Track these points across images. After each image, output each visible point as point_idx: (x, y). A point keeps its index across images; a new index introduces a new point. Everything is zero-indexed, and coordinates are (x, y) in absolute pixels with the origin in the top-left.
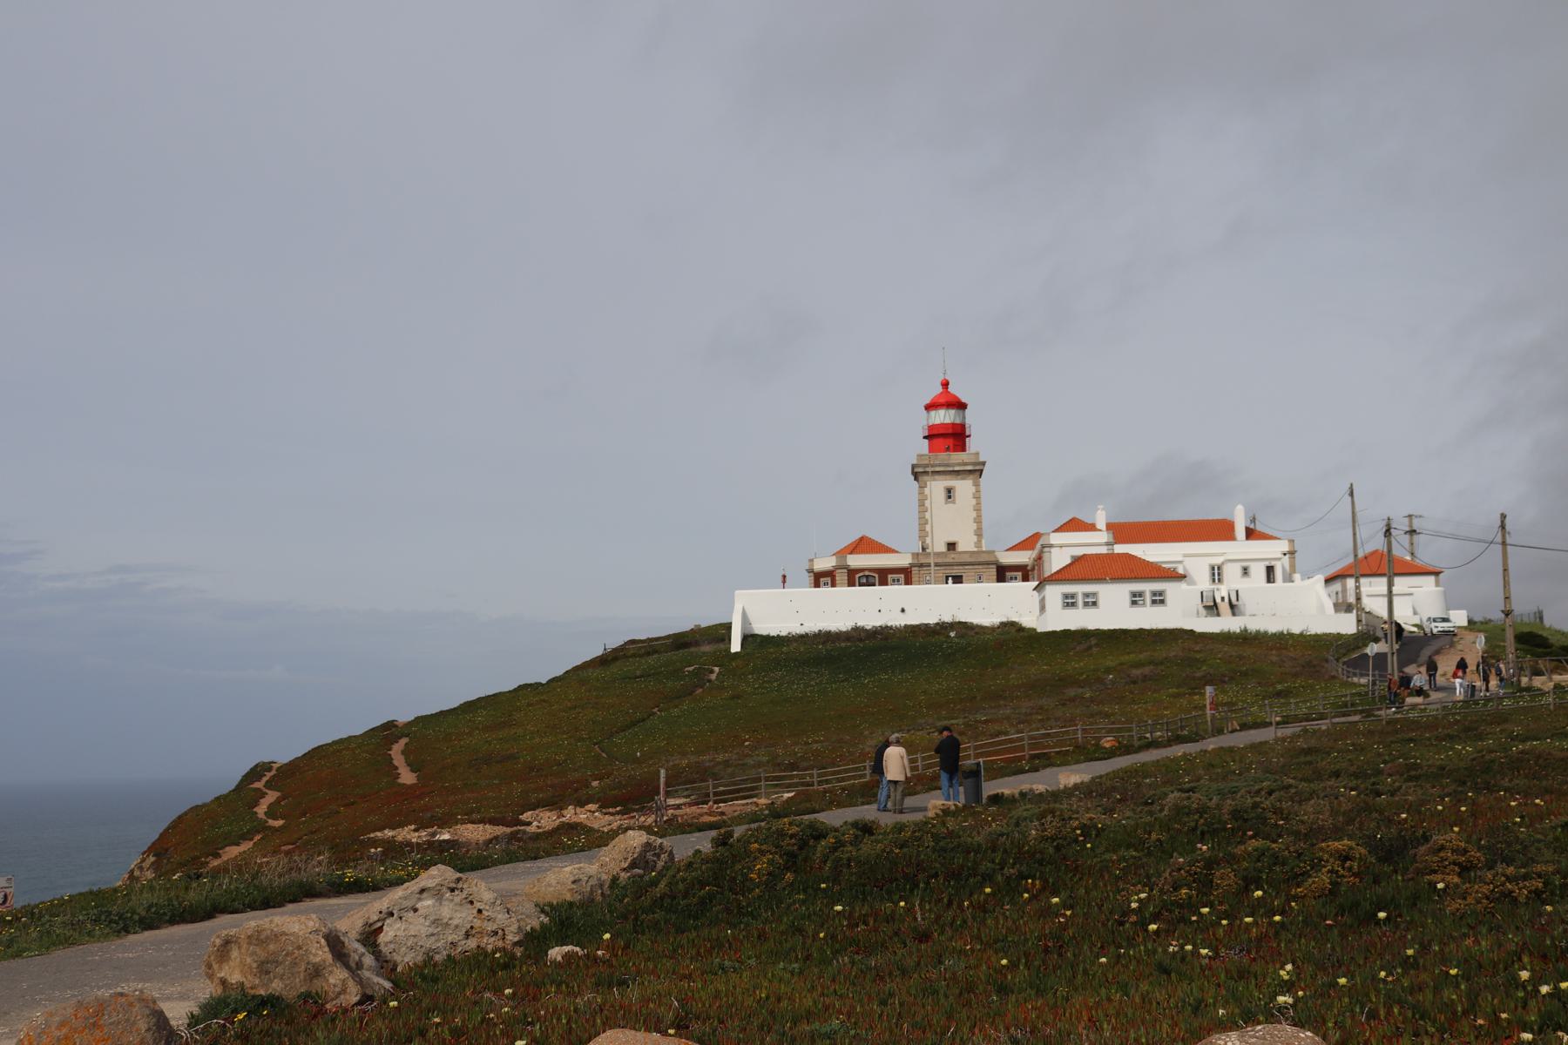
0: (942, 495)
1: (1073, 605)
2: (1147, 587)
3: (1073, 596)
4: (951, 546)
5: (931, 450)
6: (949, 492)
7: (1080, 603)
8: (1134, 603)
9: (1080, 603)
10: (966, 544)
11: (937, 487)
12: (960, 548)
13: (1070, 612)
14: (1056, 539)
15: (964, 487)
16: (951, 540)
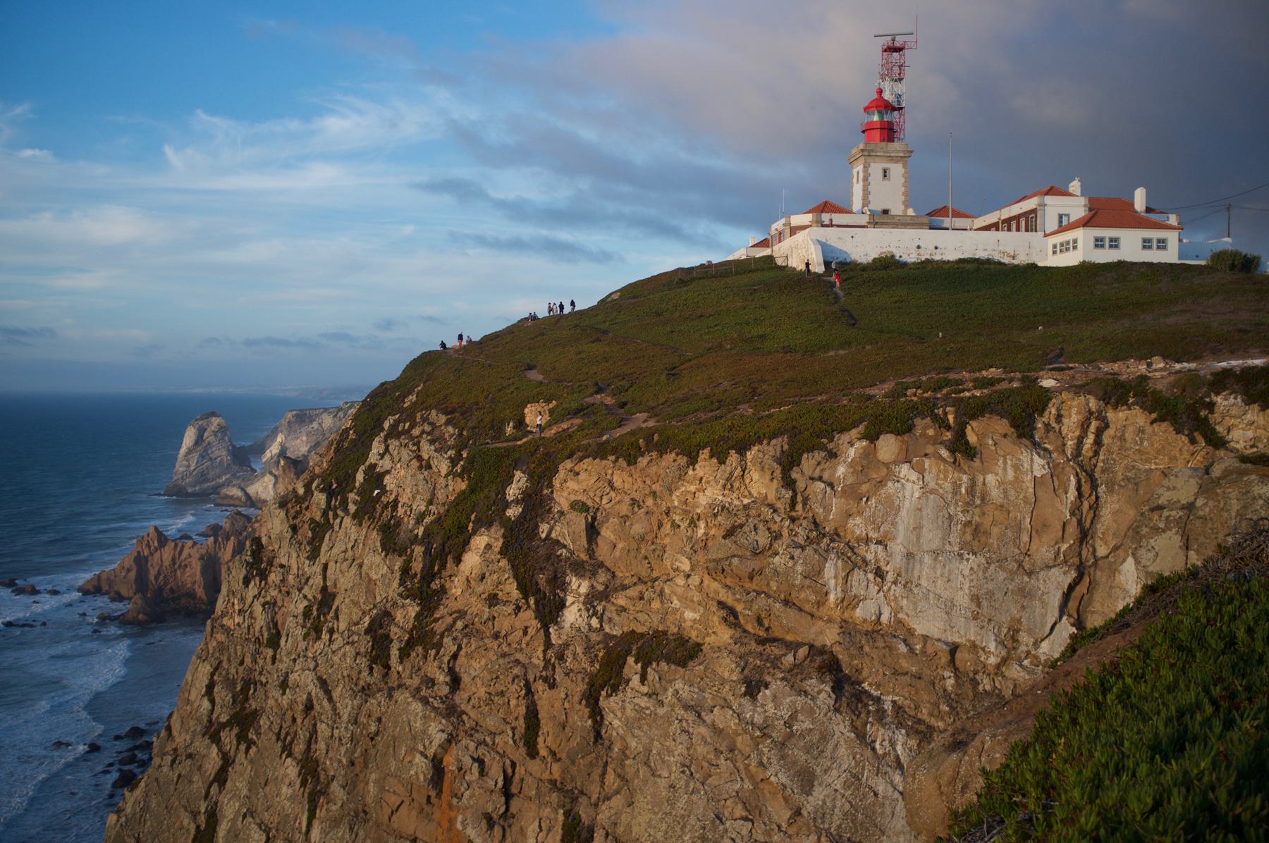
0: (881, 174)
1: (1102, 246)
2: (1154, 234)
3: (1101, 239)
4: (886, 212)
5: (869, 140)
6: (885, 173)
7: (1107, 246)
8: (1144, 247)
9: (1107, 246)
10: (897, 209)
11: (876, 168)
12: (892, 213)
13: (1100, 251)
14: (1049, 199)
15: (897, 170)
16: (886, 207)
